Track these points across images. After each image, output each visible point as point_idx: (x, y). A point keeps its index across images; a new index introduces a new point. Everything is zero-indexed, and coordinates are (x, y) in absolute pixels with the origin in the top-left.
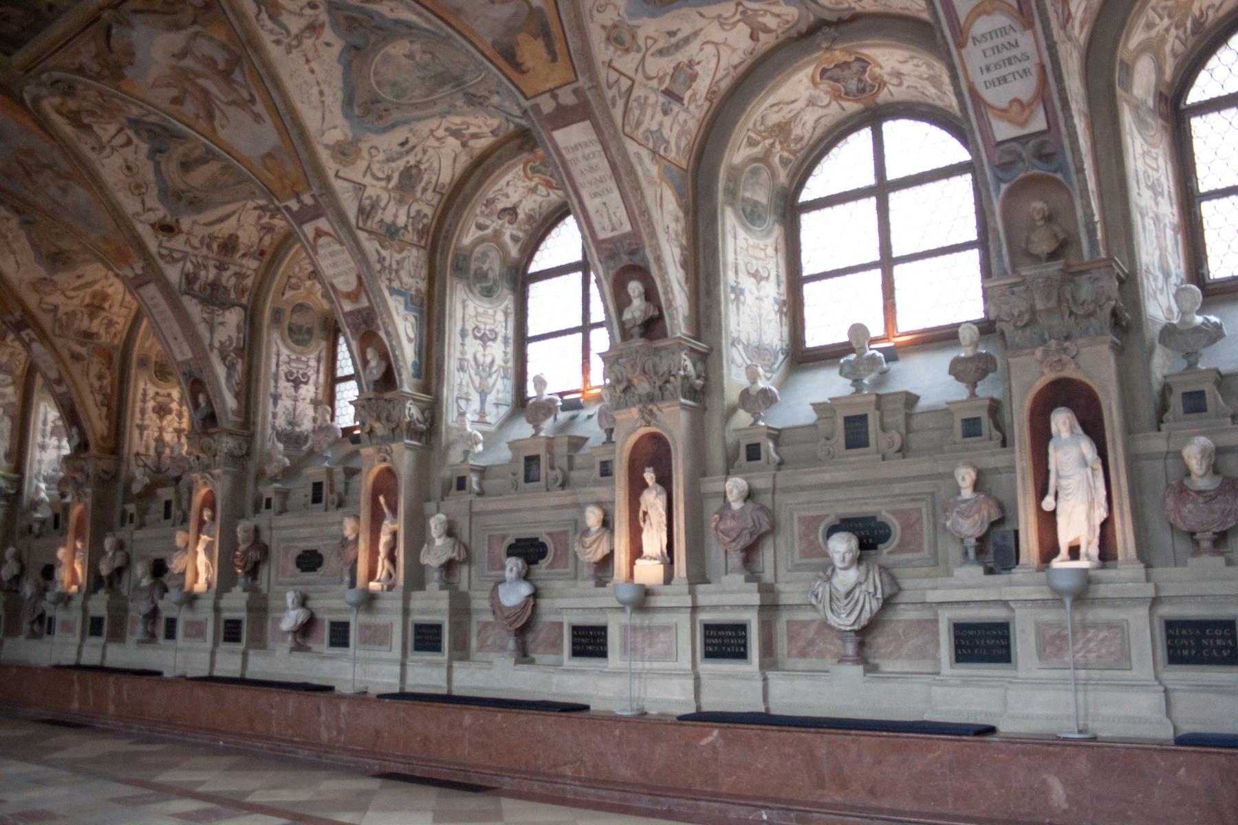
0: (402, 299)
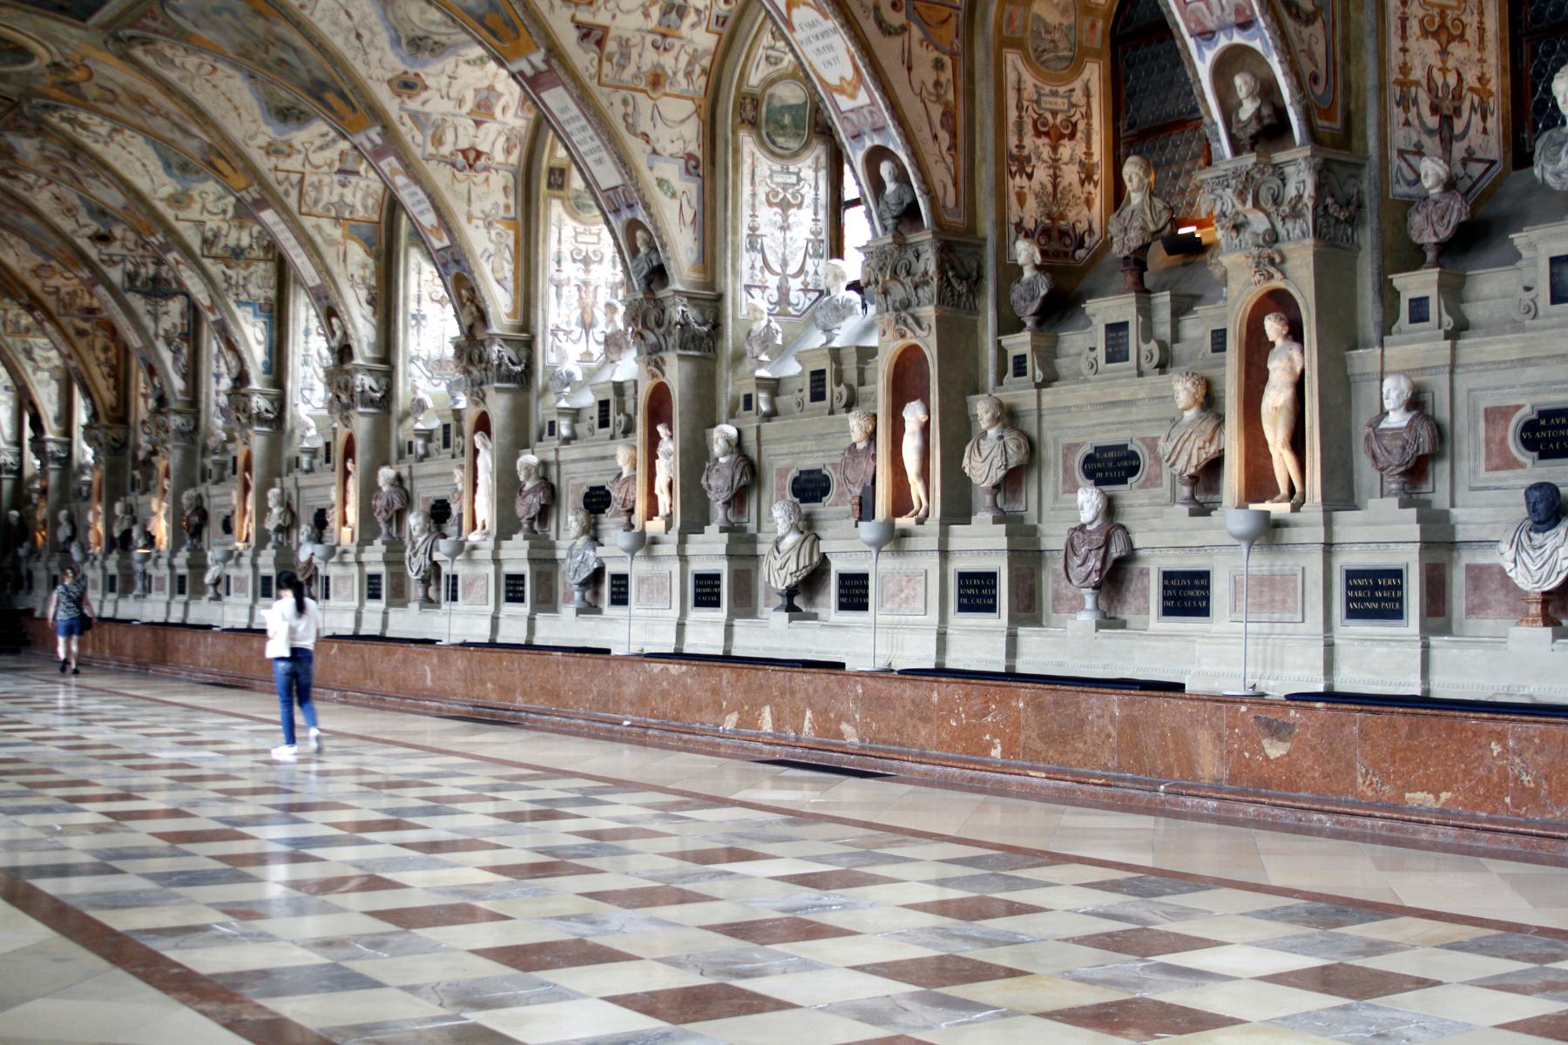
0: (250, 309)
